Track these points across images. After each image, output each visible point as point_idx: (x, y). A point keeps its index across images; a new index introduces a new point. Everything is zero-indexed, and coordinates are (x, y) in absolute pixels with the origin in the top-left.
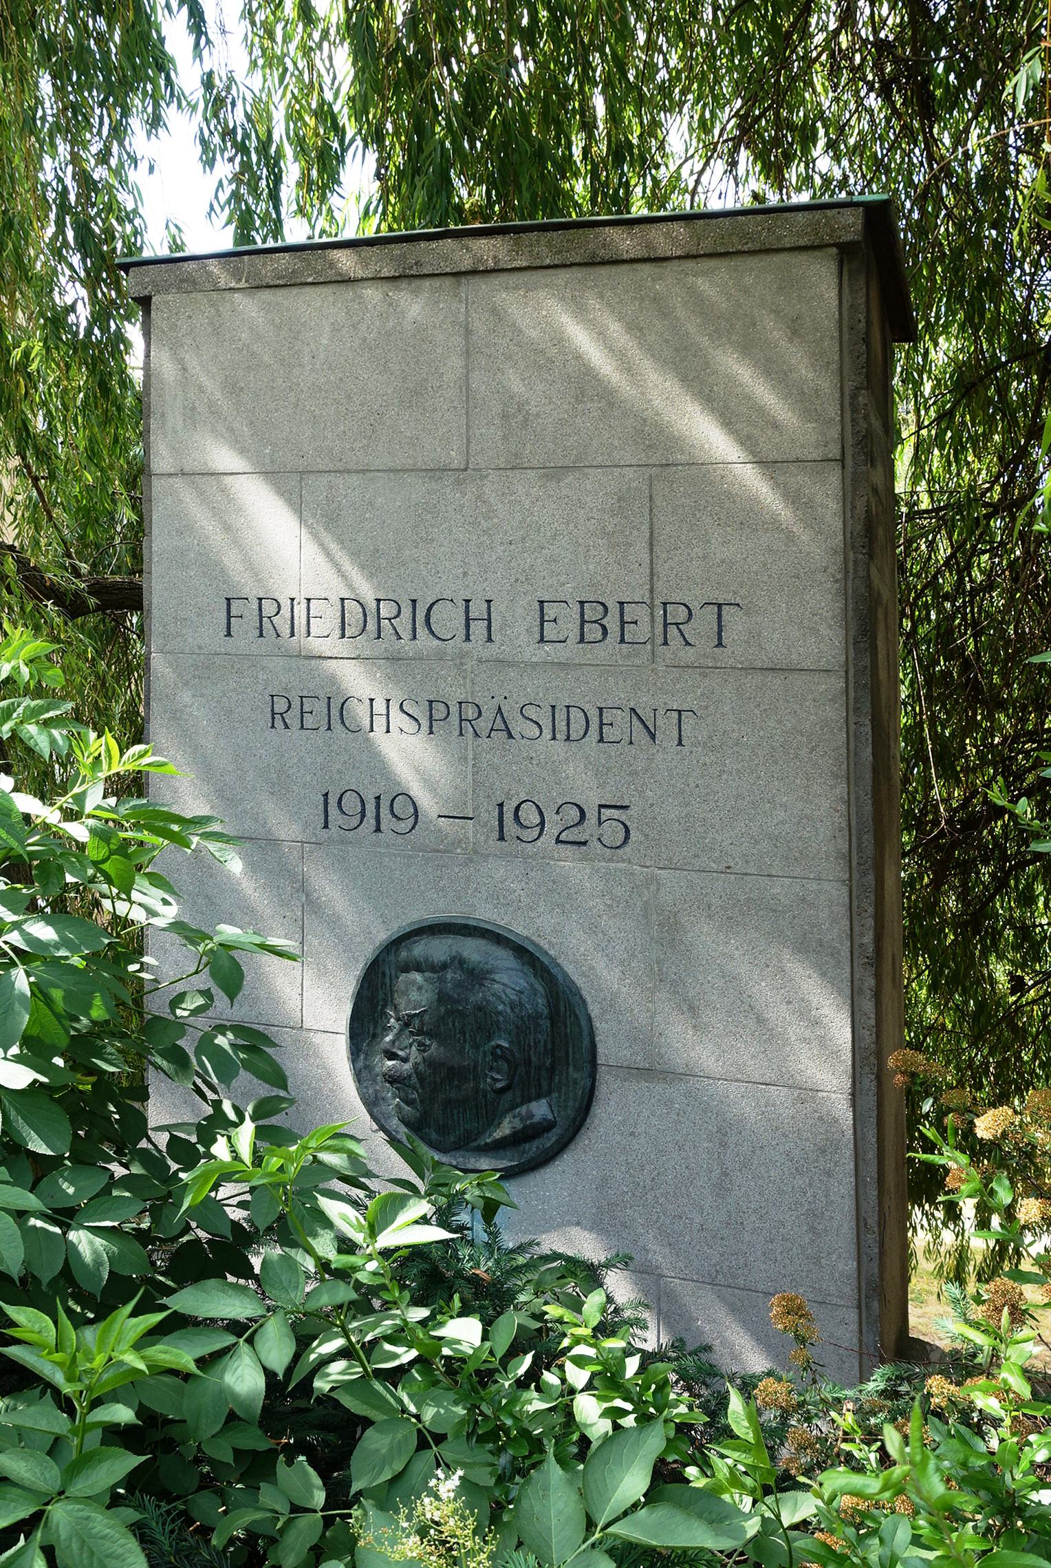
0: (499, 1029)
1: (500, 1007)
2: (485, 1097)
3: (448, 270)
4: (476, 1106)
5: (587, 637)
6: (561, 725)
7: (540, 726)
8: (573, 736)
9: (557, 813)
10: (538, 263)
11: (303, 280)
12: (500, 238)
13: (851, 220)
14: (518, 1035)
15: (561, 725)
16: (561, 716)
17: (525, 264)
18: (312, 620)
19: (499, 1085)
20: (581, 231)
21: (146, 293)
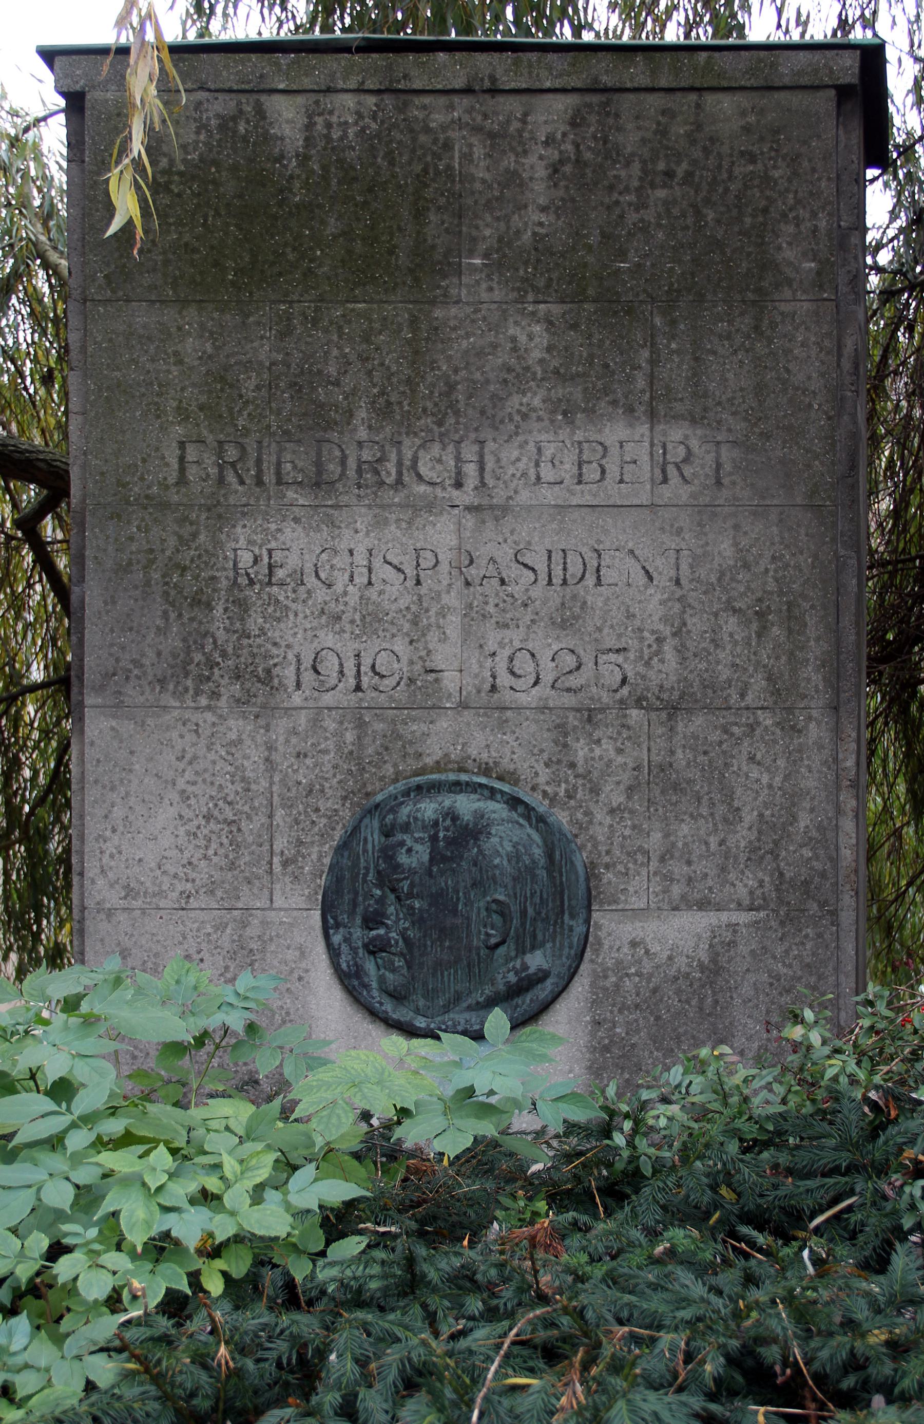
0: (495, 883)
1: (497, 861)
2: (478, 954)
3: (440, 87)
4: (469, 965)
5: (585, 478)
6: (558, 571)
7: (533, 569)
8: (570, 581)
9: (553, 660)
10: (537, 85)
11: (273, 86)
12: (496, 55)
13: (848, 63)
14: (514, 887)
15: (558, 571)
16: (557, 557)
17: (524, 86)
18: (693, 97)
19: (493, 941)
20: (582, 55)
21: (78, 88)
